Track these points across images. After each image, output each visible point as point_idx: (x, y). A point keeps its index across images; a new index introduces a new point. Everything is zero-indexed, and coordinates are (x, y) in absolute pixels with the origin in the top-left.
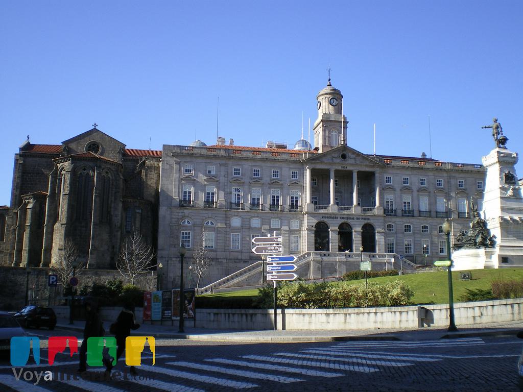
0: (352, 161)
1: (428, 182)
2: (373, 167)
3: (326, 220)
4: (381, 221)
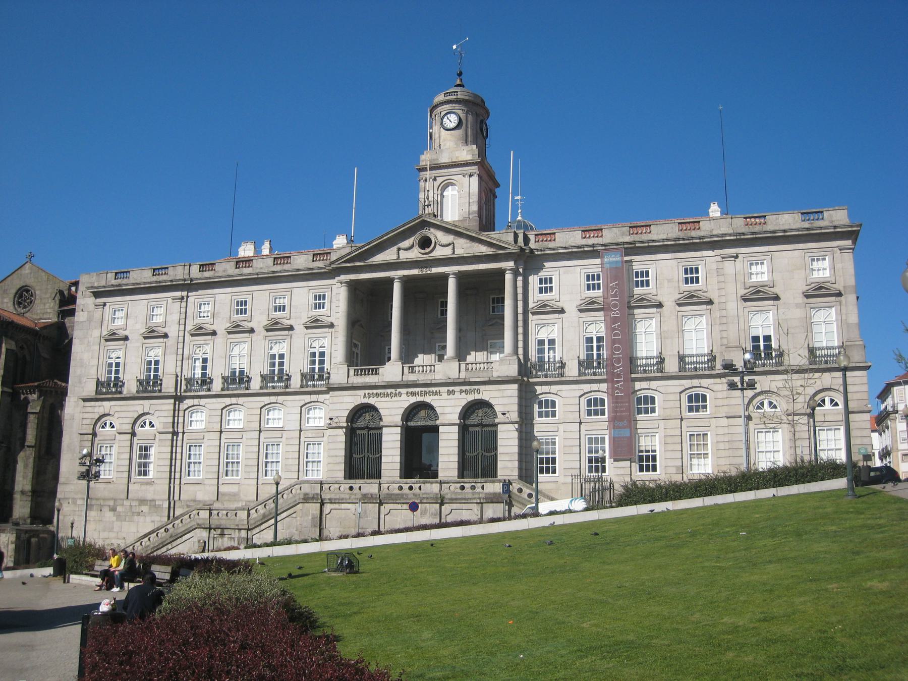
0: (446, 252)
3: (372, 401)
4: (509, 393)
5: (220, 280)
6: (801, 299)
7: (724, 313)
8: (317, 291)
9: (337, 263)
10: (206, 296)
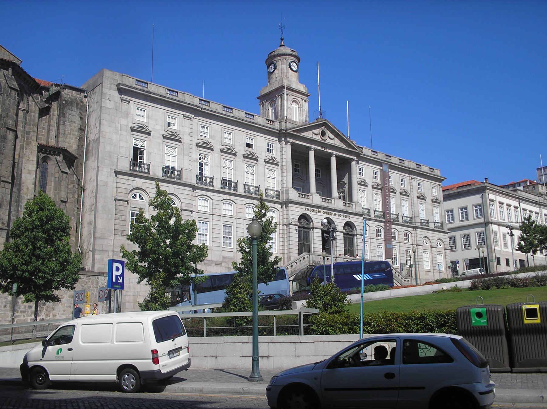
1: (394, 181)
2: (350, 153)
3: (308, 213)
4: (360, 220)
5: (219, 115)
6: (431, 202)
7: (413, 202)
8: (269, 141)
9: (290, 130)
10: (205, 122)
